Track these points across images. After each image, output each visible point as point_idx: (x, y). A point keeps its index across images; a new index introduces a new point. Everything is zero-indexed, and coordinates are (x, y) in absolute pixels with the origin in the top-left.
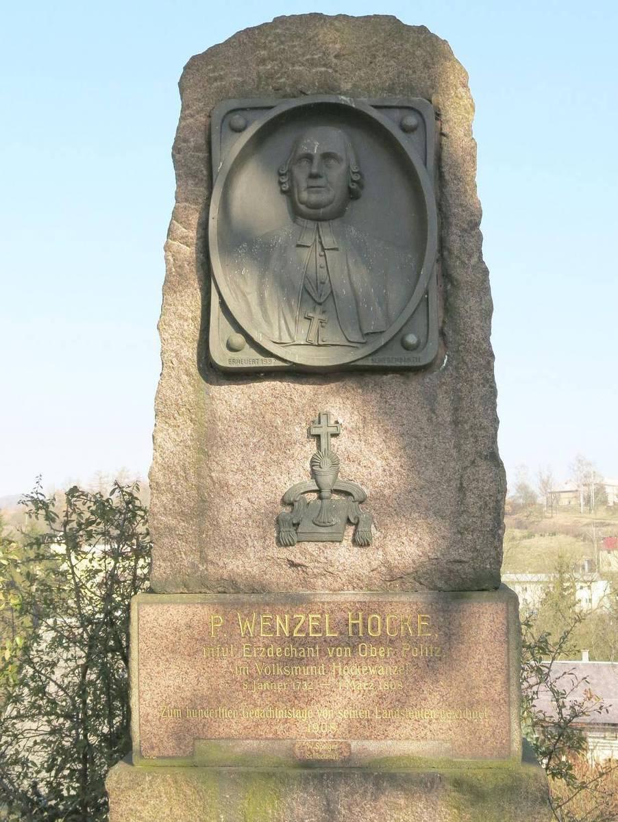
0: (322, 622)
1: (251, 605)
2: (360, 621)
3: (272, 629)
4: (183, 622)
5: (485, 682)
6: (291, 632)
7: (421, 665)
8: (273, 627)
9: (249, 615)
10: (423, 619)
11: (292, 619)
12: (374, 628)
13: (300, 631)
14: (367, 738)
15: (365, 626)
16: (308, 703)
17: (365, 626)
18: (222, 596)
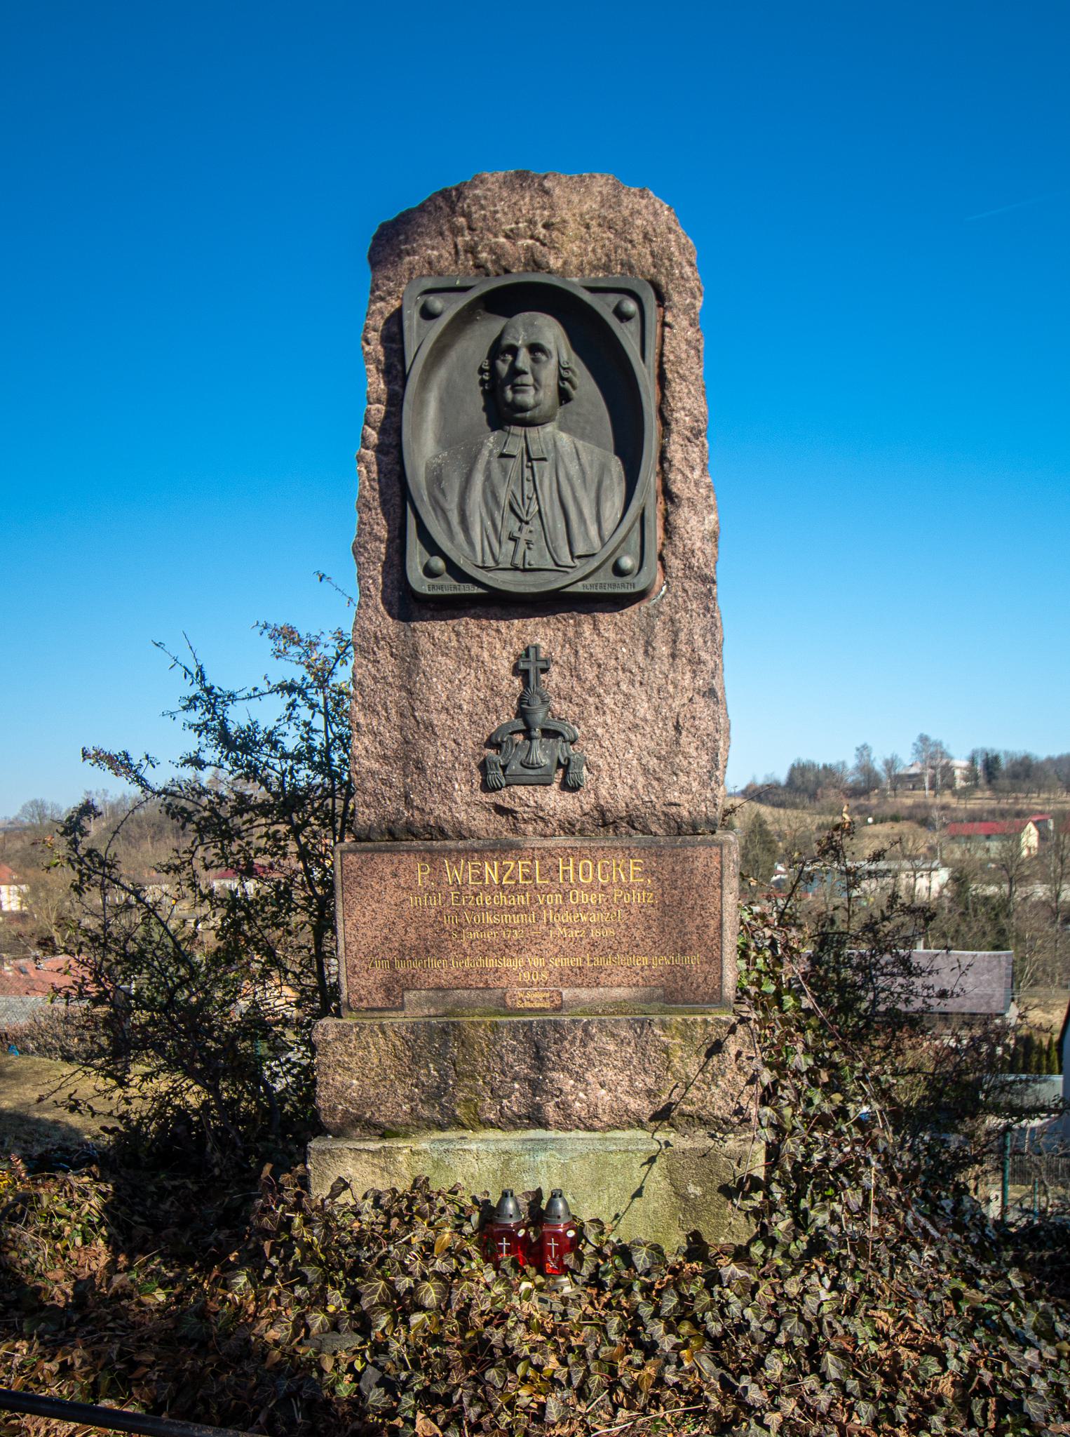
0: (532, 869)
1: (459, 851)
2: (571, 868)
3: (480, 877)
4: (388, 871)
5: (698, 928)
6: (500, 879)
7: (633, 911)
8: (482, 874)
9: (457, 862)
10: (635, 864)
11: (501, 866)
12: (585, 874)
13: (510, 878)
14: (578, 986)
15: (576, 872)
16: (519, 951)
17: (576, 872)
18: (428, 843)
